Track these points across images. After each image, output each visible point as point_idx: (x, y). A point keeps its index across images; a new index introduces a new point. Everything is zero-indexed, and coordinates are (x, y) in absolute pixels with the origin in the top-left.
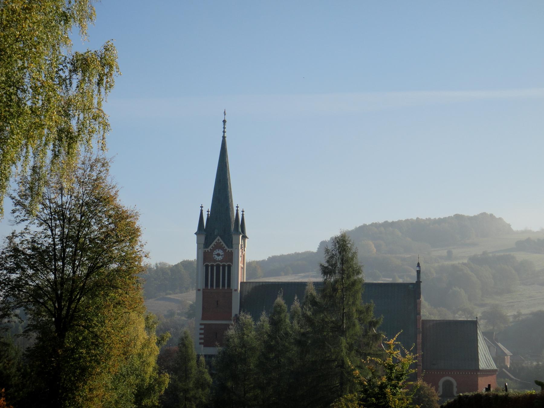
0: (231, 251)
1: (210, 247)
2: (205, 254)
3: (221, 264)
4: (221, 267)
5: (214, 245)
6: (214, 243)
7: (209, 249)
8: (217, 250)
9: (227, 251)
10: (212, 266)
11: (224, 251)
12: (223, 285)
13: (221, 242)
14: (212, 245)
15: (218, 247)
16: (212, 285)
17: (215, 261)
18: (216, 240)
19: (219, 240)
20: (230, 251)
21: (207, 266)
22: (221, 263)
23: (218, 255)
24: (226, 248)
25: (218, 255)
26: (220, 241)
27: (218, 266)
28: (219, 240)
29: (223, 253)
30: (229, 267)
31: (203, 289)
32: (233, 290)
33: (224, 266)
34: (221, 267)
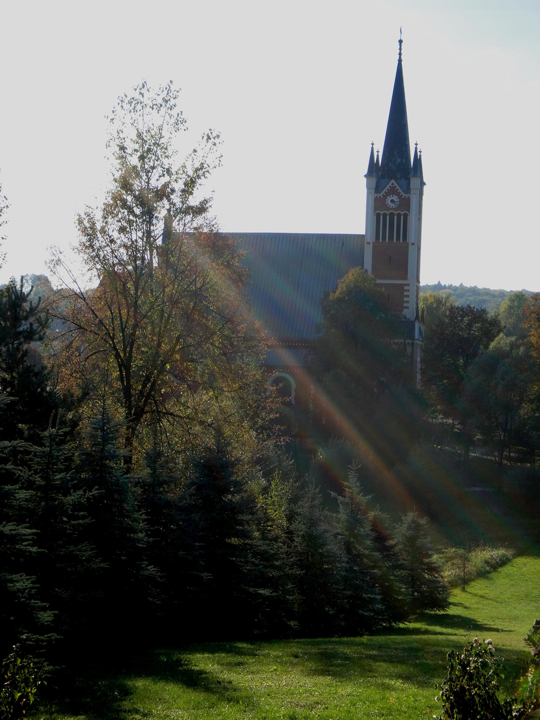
0: (408, 197)
1: (383, 192)
2: (376, 199)
3: (396, 213)
4: (396, 217)
5: (388, 189)
6: (388, 187)
7: (381, 195)
8: (391, 196)
10: (385, 215)
11: (400, 197)
12: (398, 238)
14: (385, 190)
15: (393, 191)
16: (384, 238)
17: (388, 209)
18: (390, 184)
19: (393, 184)
21: (378, 216)
23: (392, 201)
24: (402, 193)
25: (392, 201)
26: (394, 186)
27: (392, 215)
28: (393, 184)
29: (398, 200)
30: (406, 216)
31: (373, 243)
32: (410, 244)
33: (399, 216)
34: (396, 217)
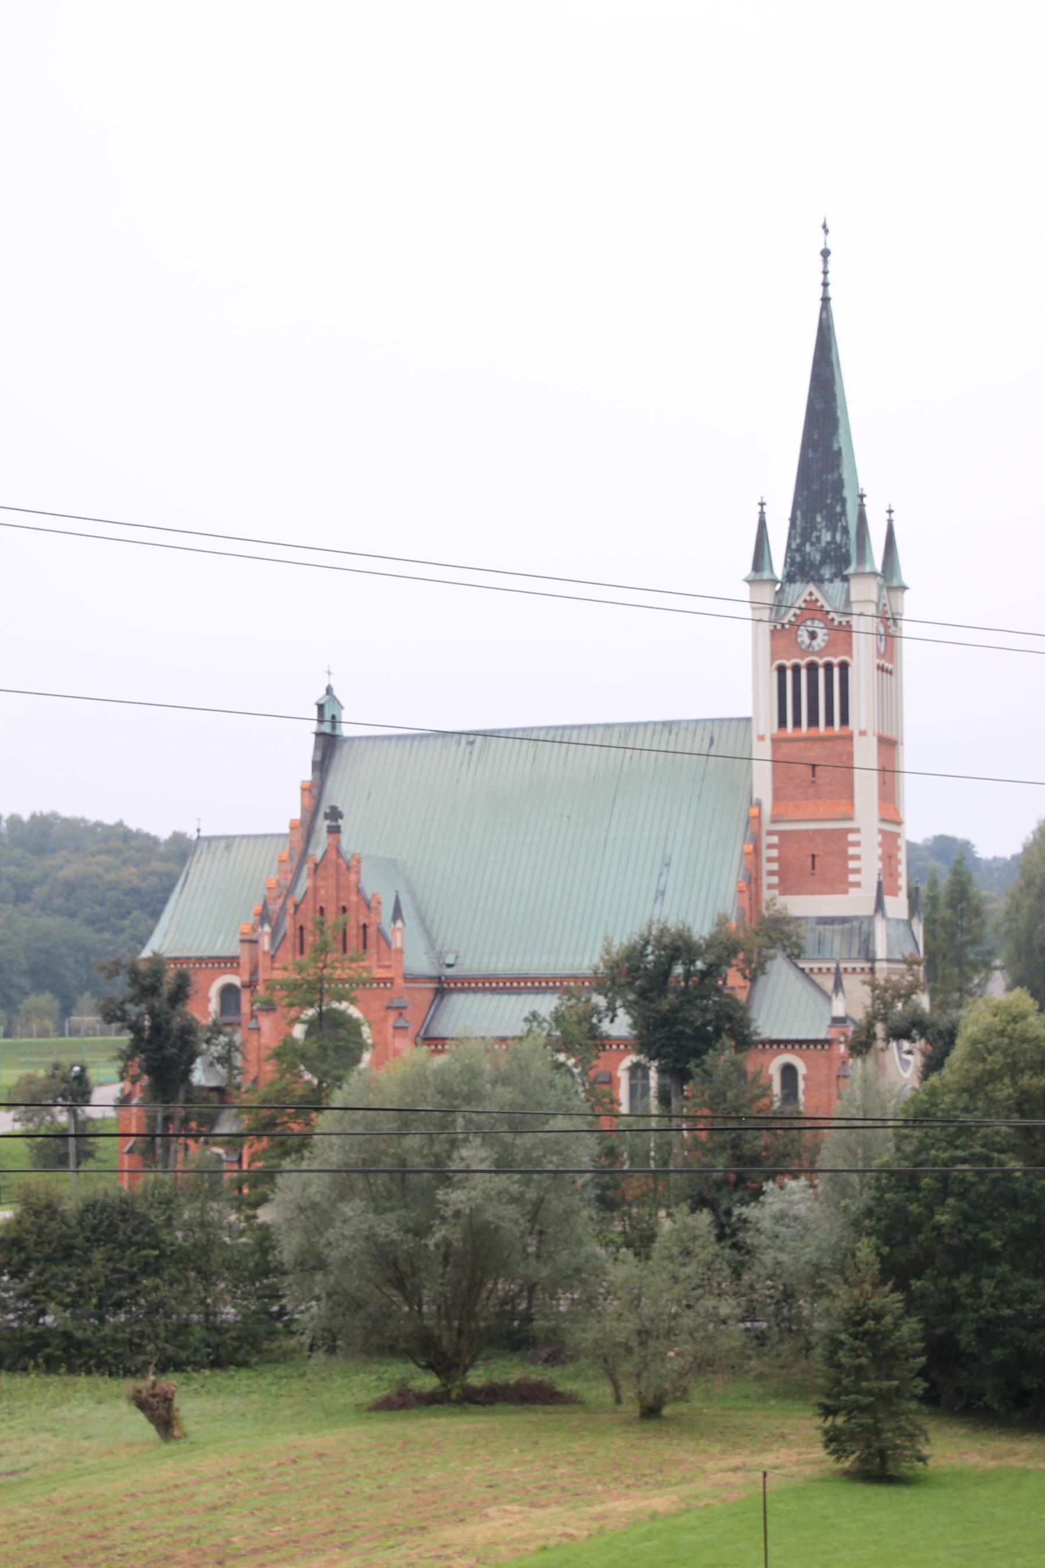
9: (836, 623)
10: (796, 669)
12: (830, 722)
13: (817, 600)
19: (811, 594)
20: (844, 623)
21: (781, 670)
22: (821, 657)
23: (813, 636)
26: (814, 598)
28: (811, 594)
30: (844, 667)
33: (829, 667)
